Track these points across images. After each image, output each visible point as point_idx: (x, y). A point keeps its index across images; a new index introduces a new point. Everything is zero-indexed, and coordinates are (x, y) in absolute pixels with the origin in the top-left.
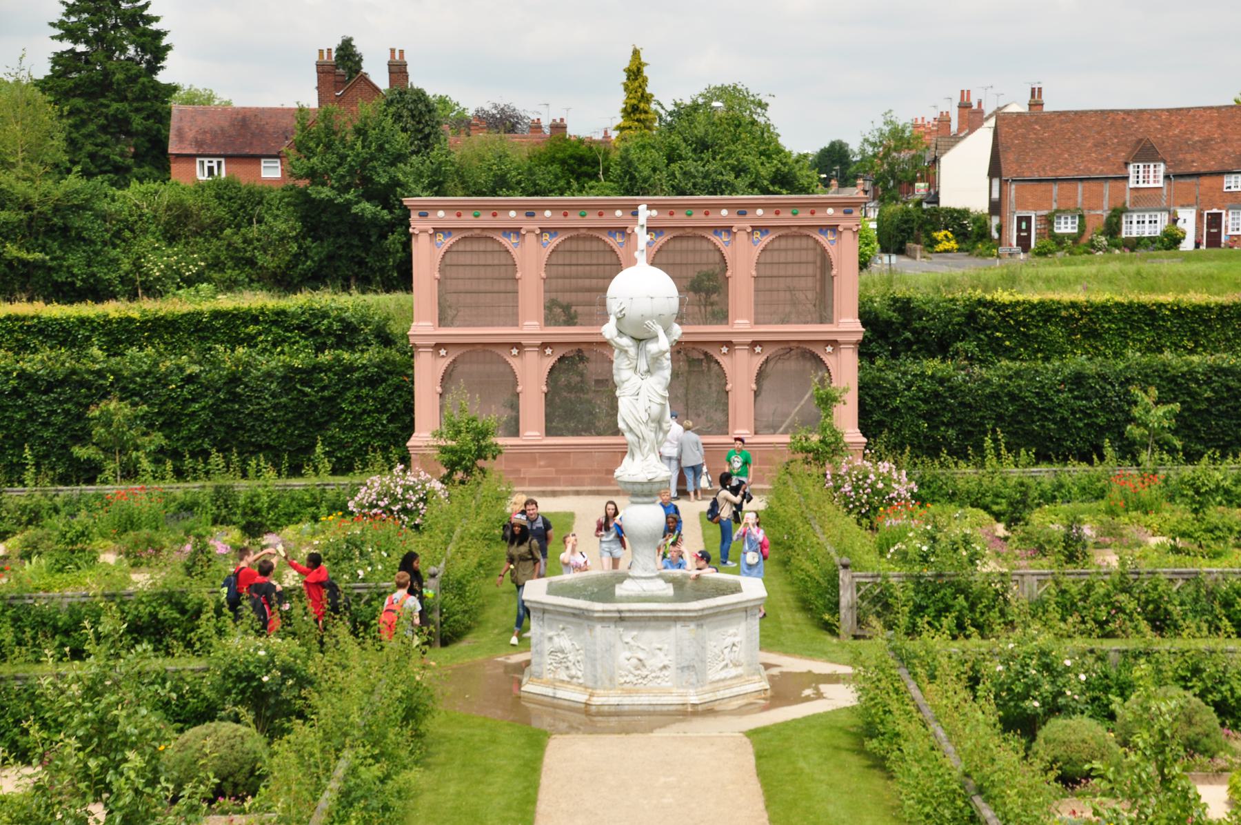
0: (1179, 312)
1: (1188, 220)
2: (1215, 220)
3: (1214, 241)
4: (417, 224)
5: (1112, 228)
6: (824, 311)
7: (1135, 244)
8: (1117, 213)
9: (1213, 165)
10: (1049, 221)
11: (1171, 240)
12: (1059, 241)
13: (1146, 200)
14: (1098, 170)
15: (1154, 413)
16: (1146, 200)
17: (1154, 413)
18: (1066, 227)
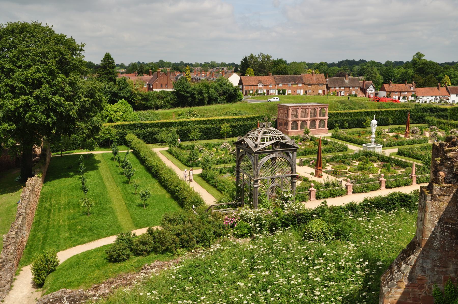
0: (341, 113)
1: (265, 91)
2: (268, 91)
3: (268, 94)
4: (290, 108)
5: (257, 92)
6: (324, 115)
7: (259, 94)
8: (257, 90)
9: (268, 84)
10: (249, 91)
11: (264, 94)
12: (251, 94)
13: (260, 88)
14: (255, 84)
15: (346, 124)
16: (260, 88)
17: (346, 124)
18: (251, 92)
